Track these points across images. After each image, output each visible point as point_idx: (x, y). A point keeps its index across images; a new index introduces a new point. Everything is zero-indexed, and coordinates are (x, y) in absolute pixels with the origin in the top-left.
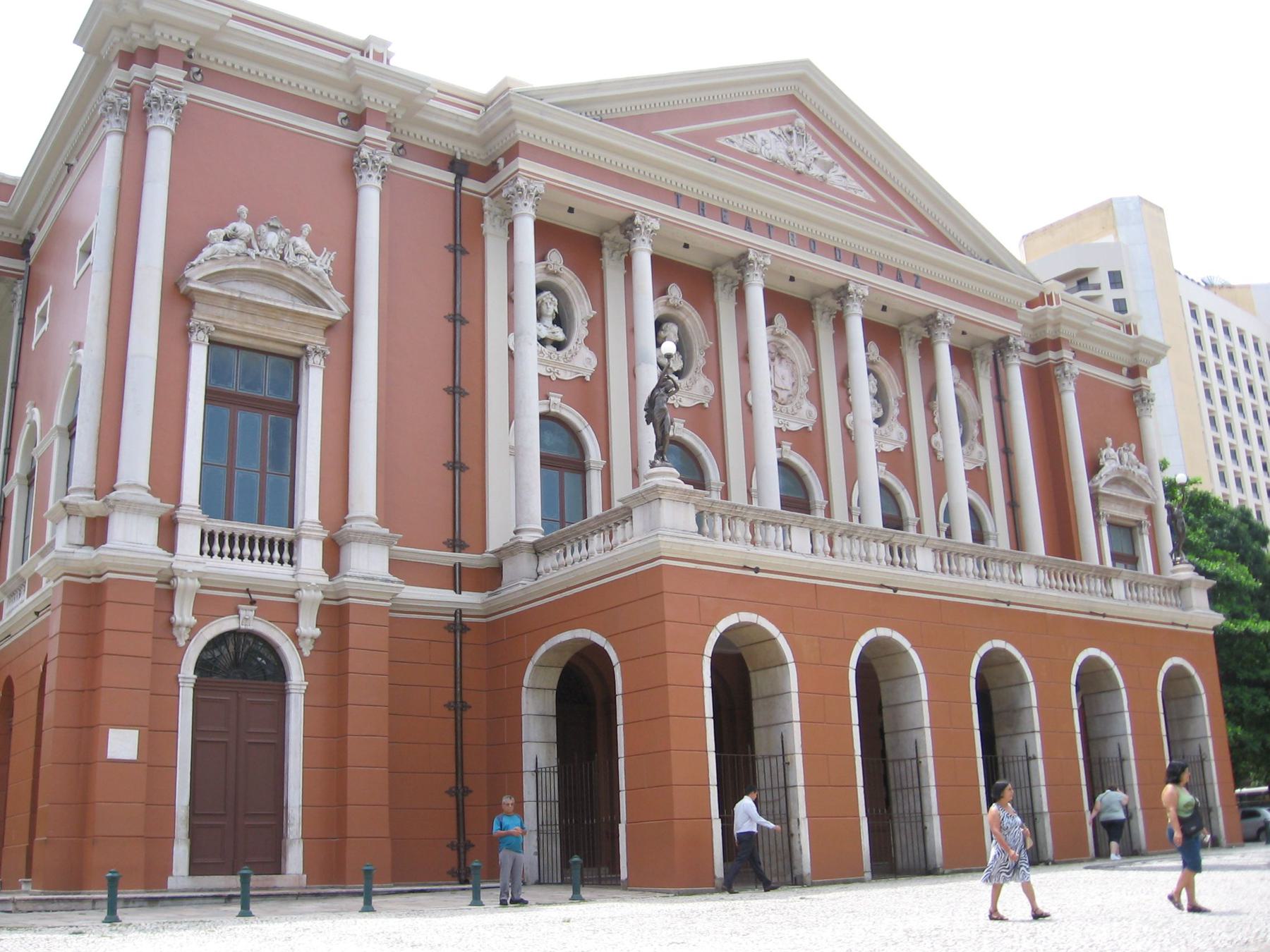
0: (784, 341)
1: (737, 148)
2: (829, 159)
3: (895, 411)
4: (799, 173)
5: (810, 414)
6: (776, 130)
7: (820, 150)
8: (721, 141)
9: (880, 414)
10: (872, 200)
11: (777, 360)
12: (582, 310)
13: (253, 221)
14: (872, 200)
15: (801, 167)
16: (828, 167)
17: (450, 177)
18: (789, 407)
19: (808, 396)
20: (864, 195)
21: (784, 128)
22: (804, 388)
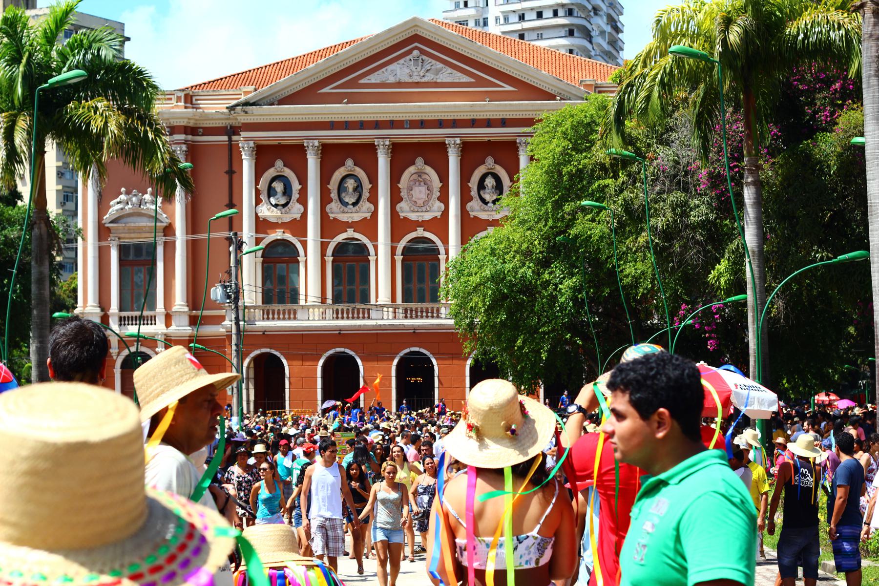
1: (373, 81)
2: (440, 65)
4: (418, 83)
6: (402, 61)
7: (434, 62)
8: (362, 81)
9: (495, 198)
10: (473, 80)
12: (296, 186)
13: (128, 193)
14: (473, 80)
15: (416, 79)
16: (438, 72)
17: (226, 138)
20: (465, 79)
21: (408, 58)
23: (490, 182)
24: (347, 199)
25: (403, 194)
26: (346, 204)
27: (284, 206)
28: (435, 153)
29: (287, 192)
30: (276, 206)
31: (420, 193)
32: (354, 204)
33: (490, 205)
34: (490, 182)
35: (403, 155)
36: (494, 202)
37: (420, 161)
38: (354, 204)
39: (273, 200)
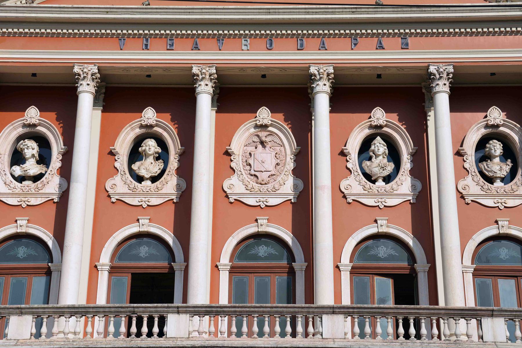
0: (270, 129)
3: (406, 164)
5: (295, 186)
11: (260, 146)
18: (270, 186)
19: (295, 172)
22: (290, 165)
23: (379, 146)
24: (143, 173)
25: (237, 163)
26: (140, 179)
27: (36, 178)
28: (290, 97)
29: (44, 159)
30: (21, 179)
31: (266, 159)
32: (154, 179)
33: (380, 183)
34: (379, 146)
35: (237, 94)
36: (388, 179)
37: (264, 115)
38: (154, 179)
39: (18, 170)
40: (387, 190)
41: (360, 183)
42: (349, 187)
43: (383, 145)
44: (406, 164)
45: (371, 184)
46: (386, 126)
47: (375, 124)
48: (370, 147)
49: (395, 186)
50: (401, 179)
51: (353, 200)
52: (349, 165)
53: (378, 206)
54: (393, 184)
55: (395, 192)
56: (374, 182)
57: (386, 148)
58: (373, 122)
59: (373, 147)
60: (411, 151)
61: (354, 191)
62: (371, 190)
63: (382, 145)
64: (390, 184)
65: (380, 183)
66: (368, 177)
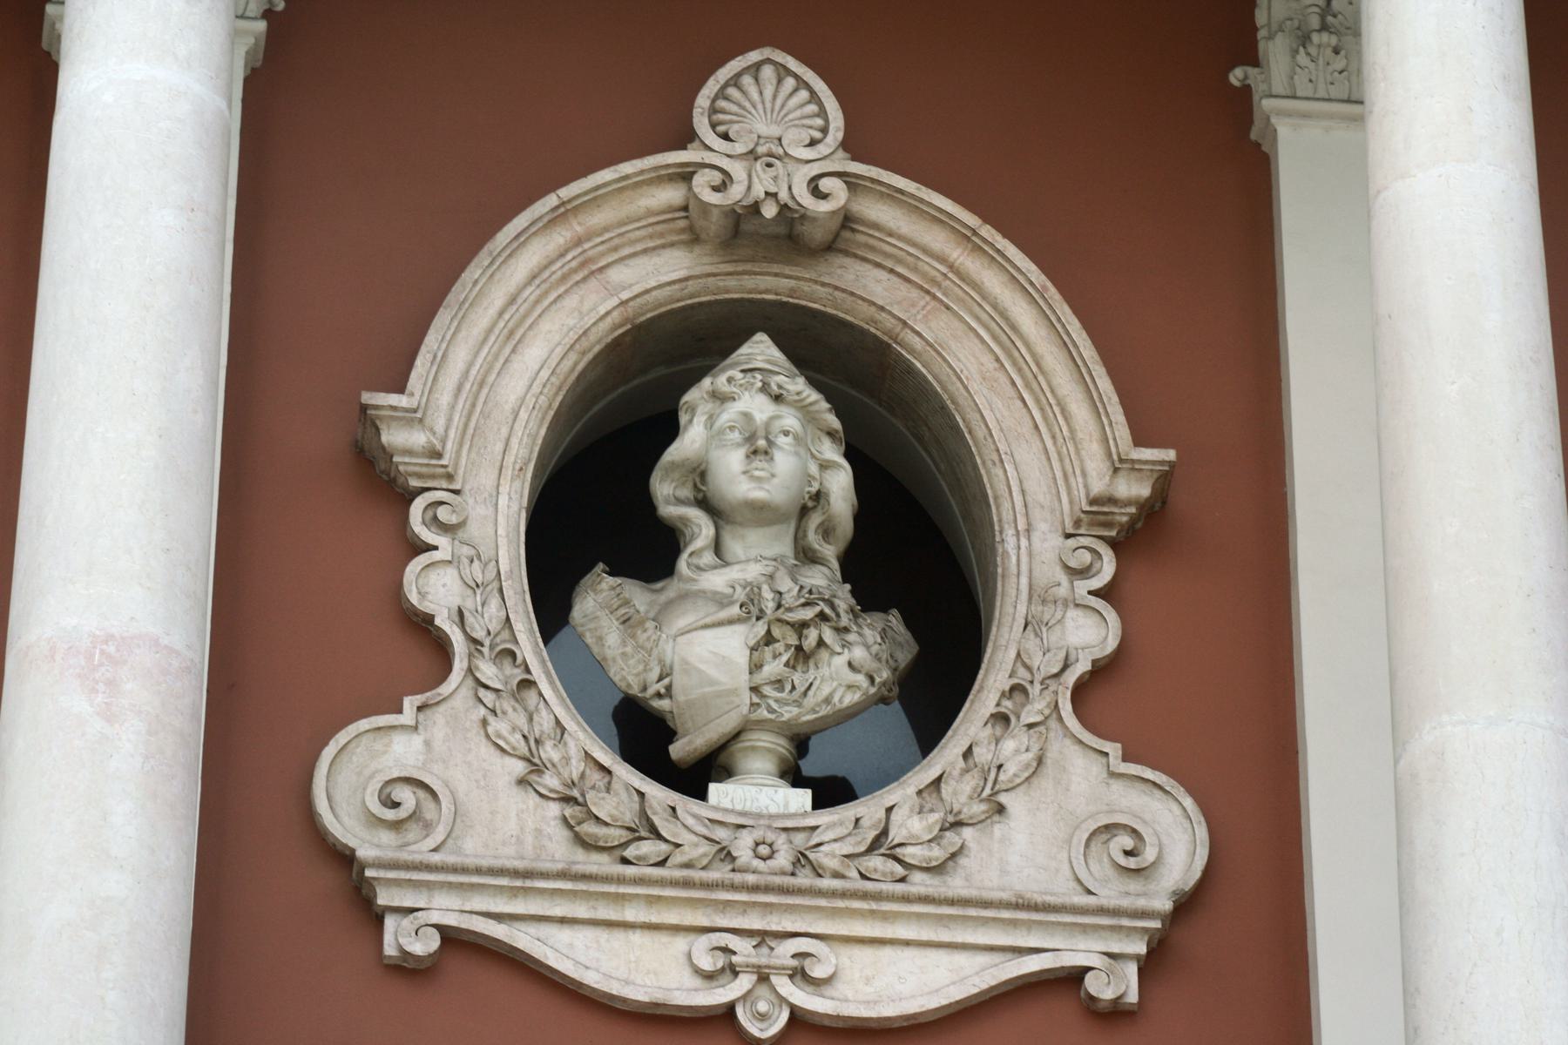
33: (757, 794)
40: (828, 857)
41: (537, 767)
42: (406, 795)
43: (804, 409)
44: (1050, 609)
45: (658, 794)
46: (844, 235)
47: (736, 192)
48: (669, 429)
49: (911, 825)
50: (982, 755)
51: (451, 938)
52: (435, 588)
53: (728, 1012)
54: (900, 806)
55: (921, 883)
56: (693, 779)
57: (832, 452)
58: (702, 181)
59: (690, 441)
60: (1098, 486)
61: (473, 848)
62: (648, 848)
63: (791, 420)
64: (868, 809)
65: (757, 794)
66: (642, 733)
